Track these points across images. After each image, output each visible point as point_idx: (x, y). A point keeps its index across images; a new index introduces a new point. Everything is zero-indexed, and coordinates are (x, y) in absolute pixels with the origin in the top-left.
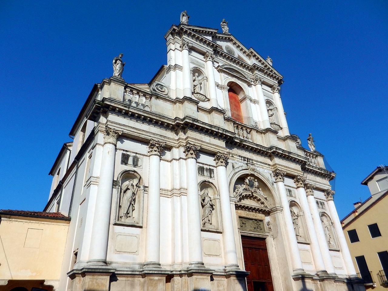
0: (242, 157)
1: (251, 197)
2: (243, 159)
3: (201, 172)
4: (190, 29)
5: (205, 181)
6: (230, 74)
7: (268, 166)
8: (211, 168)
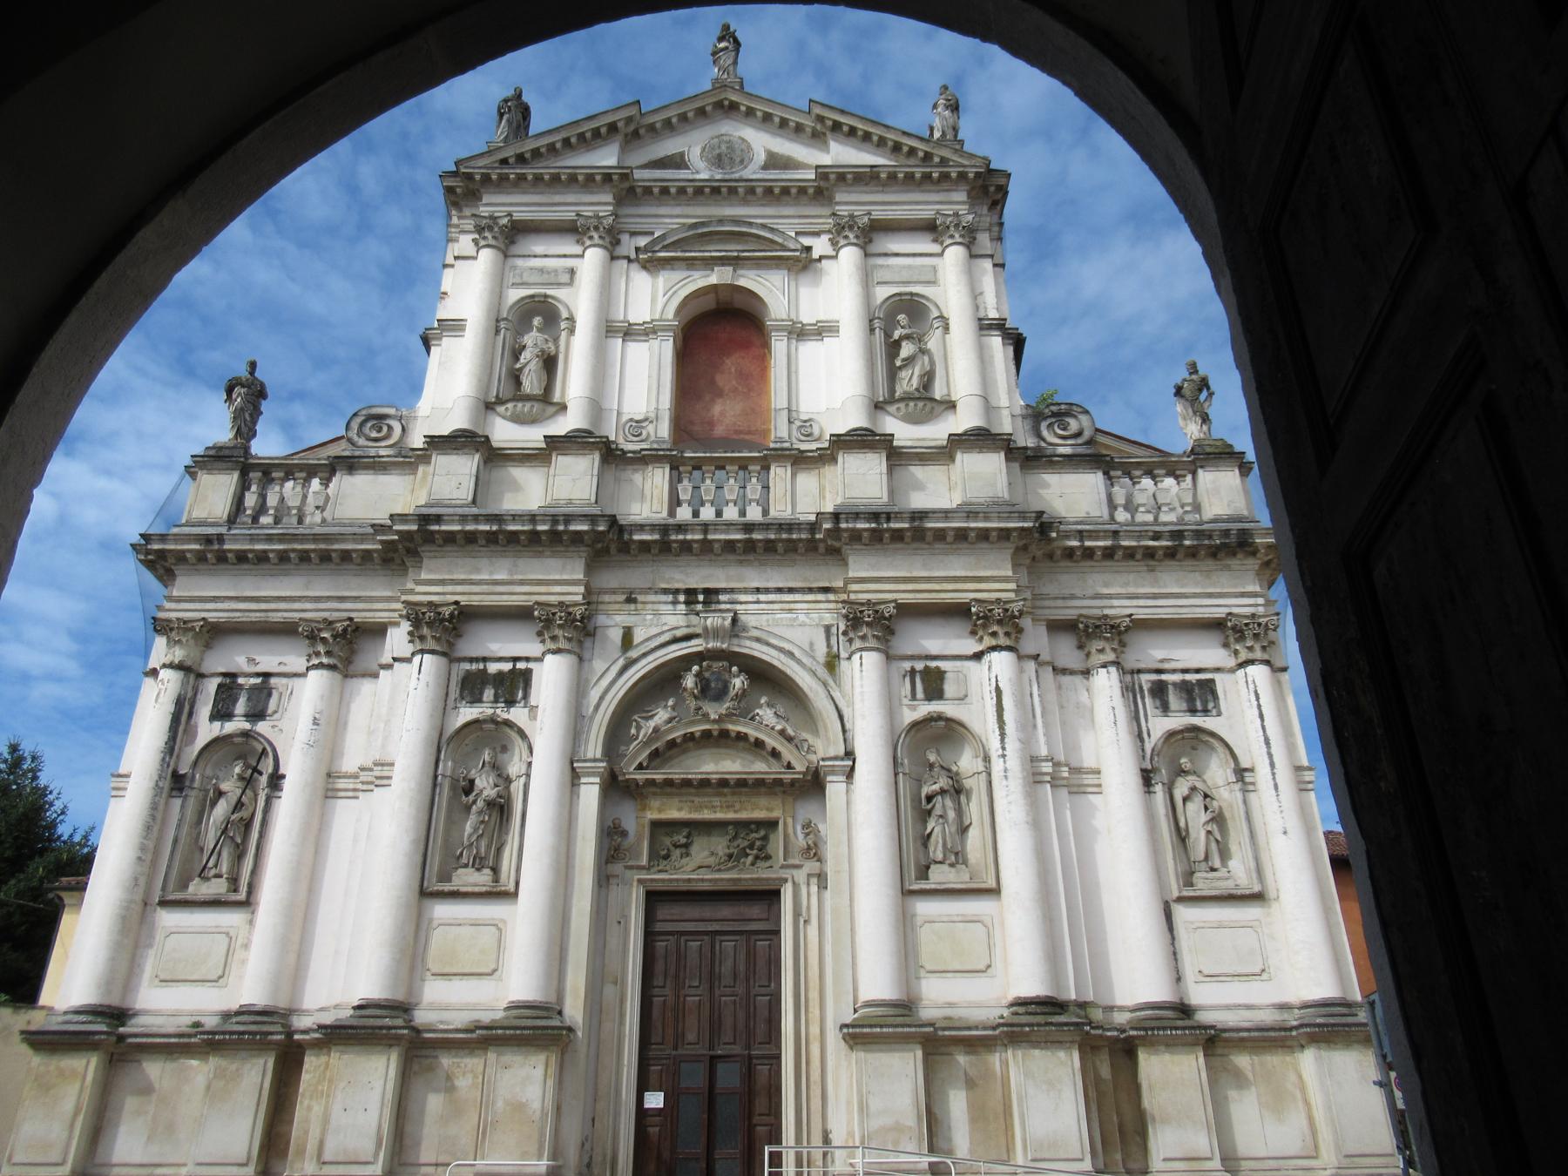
0: (676, 592)
1: (720, 739)
2: (682, 598)
4: (504, 162)
5: (476, 721)
7: (820, 597)
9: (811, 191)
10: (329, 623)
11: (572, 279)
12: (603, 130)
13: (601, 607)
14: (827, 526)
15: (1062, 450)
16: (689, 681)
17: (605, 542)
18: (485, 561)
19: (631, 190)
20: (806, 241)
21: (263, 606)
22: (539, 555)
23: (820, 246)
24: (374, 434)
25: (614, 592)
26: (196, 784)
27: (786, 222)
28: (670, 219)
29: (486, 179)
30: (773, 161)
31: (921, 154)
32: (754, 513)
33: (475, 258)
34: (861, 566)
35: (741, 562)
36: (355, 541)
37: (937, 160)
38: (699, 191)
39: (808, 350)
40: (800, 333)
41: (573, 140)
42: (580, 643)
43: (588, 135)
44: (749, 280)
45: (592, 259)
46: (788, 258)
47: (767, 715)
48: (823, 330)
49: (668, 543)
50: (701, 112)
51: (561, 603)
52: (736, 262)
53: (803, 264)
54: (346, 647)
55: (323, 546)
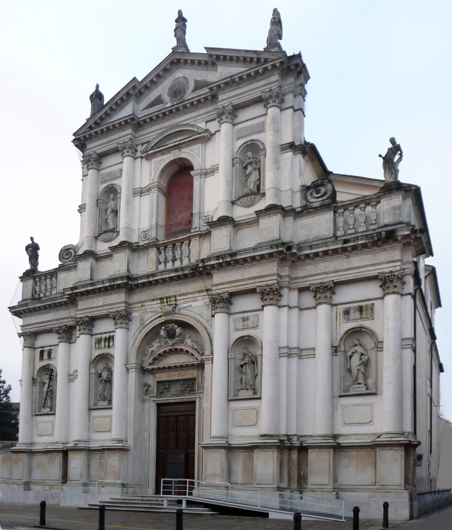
8: (111, 334)
9: (209, 98)
12: (124, 97)
13: (134, 309)
17: (129, 284)
23: (213, 126)
25: (137, 303)
26: (38, 381)
27: (197, 120)
29: (85, 137)
32: (186, 262)
35: (178, 284)
36: (50, 301)
41: (114, 107)
42: (126, 324)
43: (119, 102)
46: (200, 138)
49: (151, 282)
50: (166, 70)
53: (206, 137)
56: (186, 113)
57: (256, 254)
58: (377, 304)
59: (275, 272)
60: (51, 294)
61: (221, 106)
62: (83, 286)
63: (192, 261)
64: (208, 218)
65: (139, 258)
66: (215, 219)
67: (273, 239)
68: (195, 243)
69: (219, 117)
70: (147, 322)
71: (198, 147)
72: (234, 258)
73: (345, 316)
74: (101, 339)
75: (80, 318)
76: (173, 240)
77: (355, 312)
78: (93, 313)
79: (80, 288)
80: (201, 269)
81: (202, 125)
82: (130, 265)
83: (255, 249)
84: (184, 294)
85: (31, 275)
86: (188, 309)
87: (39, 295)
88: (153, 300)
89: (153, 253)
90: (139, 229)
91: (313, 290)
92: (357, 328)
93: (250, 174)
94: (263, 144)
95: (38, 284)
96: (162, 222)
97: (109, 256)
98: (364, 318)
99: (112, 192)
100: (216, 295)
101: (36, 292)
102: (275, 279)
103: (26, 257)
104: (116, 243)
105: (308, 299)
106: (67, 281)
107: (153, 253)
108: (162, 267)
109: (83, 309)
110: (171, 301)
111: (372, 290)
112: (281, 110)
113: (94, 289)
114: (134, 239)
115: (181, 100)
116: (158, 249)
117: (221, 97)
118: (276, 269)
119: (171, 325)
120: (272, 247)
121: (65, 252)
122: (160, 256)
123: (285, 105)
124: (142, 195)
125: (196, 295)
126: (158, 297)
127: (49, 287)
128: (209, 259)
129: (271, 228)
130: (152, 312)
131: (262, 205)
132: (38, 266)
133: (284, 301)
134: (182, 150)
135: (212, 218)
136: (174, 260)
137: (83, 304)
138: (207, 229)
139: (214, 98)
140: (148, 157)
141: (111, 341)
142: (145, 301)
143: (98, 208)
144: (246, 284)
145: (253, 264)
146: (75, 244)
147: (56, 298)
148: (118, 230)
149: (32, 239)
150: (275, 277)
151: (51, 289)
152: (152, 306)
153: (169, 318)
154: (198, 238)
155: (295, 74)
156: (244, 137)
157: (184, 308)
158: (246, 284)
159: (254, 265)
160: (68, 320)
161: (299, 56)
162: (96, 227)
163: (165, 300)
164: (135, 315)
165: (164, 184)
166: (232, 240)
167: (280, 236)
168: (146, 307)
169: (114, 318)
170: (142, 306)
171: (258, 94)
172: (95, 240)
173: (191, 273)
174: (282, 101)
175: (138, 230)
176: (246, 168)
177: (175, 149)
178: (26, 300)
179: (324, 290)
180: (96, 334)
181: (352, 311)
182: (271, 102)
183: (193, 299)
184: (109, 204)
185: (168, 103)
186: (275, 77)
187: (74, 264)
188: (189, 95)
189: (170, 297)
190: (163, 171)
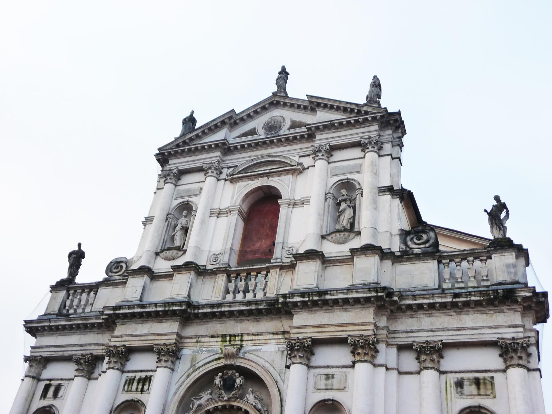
3: (129, 385)
6: (251, 176)
8: (149, 374)
9: (306, 136)
10: (83, 356)
11: (200, 193)
13: (186, 345)
14: (280, 301)
15: (416, 251)
16: (217, 381)
17: (187, 313)
18: (140, 325)
19: (229, 148)
20: (302, 160)
21: (63, 349)
22: (161, 321)
23: (307, 162)
24: (115, 271)
25: (191, 337)
28: (241, 160)
30: (295, 125)
31: (356, 111)
32: (260, 296)
33: (163, 188)
34: (300, 319)
35: (248, 320)
36: (82, 320)
37: (363, 112)
38: (264, 143)
39: (297, 211)
40: (294, 204)
42: (172, 362)
44: (273, 182)
45: (211, 180)
47: (251, 397)
48: (303, 202)
49: (216, 313)
51: (165, 344)
52: (268, 175)
53: (298, 170)
54: (89, 365)
55: (84, 322)
56: (279, 146)
57: (350, 296)
58: (498, 377)
59: (372, 320)
60: (83, 312)
61: (318, 145)
62: (129, 307)
63: (267, 295)
64: (293, 250)
65: (203, 283)
66: (301, 251)
67: (369, 282)
68: (274, 275)
69: (314, 153)
70: (200, 364)
71: (288, 178)
72: (323, 298)
73: (457, 389)
74: (134, 379)
75: (115, 346)
76: (249, 268)
77: (470, 385)
78: (133, 343)
79: (126, 308)
80: (280, 306)
81: (296, 159)
82: (192, 290)
83: (349, 290)
84: (253, 334)
85: (66, 285)
86: (255, 353)
87: (68, 310)
88: (213, 336)
89: (222, 279)
90: (210, 251)
91: (416, 350)
92: (475, 407)
93: (344, 210)
94: (359, 184)
95: (70, 297)
96: (237, 247)
97: (168, 276)
98: (483, 395)
99: (186, 208)
100: (295, 340)
101: (65, 307)
102: (371, 330)
103: (66, 264)
104: (180, 262)
105: (409, 361)
106: (108, 298)
107: (222, 279)
108: (229, 298)
109: (122, 336)
110: (235, 341)
111: (490, 359)
112: (379, 156)
113: (142, 312)
114: (202, 261)
115: (275, 135)
116: (229, 276)
117: (317, 137)
118: (372, 317)
119: (230, 372)
120: (370, 291)
121: (115, 265)
122: (229, 285)
123: (382, 153)
124: (219, 216)
125: (268, 337)
126: (219, 333)
127: (83, 303)
128: (292, 295)
129: (368, 269)
130: (209, 351)
131: (357, 243)
132: (77, 277)
133: (380, 359)
134: (271, 179)
135: (297, 251)
136: (246, 291)
137: (121, 329)
138: (291, 261)
139: (310, 136)
140: (233, 181)
141: (147, 383)
142: (202, 337)
143: (167, 223)
144: (334, 332)
145: (344, 307)
146: (129, 257)
147: (89, 318)
148: (184, 248)
149: (80, 245)
150: (372, 327)
151: (85, 305)
152: (211, 344)
153: (229, 362)
154: (278, 270)
155: (394, 128)
156: (339, 174)
157: (250, 352)
158: (334, 332)
159: (346, 309)
160: (96, 348)
161: (399, 113)
162: (159, 242)
163: (228, 339)
164: (186, 352)
165: (245, 208)
166: (320, 277)
167: (377, 279)
168: (202, 344)
169: (159, 353)
170: (197, 342)
171: (357, 139)
172: (154, 256)
173: (267, 309)
174: (381, 148)
175: (208, 252)
176: (339, 204)
177: (264, 177)
178: (50, 314)
179: (431, 352)
180: (128, 372)
181: (466, 383)
182: (370, 147)
183: (264, 341)
184: (179, 222)
185: (262, 135)
186: (375, 127)
187: (123, 279)
188: (284, 131)
189: (235, 335)
190: (247, 195)
